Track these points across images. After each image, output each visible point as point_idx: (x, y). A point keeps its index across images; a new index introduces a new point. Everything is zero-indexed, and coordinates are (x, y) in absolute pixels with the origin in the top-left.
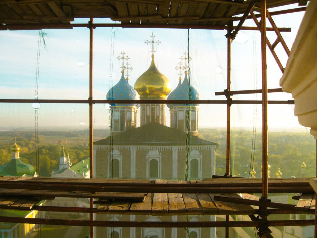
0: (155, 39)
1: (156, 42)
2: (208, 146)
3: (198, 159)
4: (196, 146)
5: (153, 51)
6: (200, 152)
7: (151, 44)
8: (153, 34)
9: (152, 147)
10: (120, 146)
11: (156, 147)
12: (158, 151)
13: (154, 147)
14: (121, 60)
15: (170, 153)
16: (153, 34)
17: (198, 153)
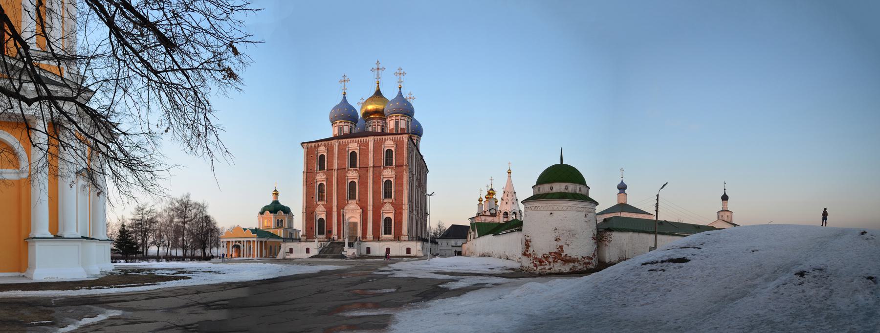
0: (380, 66)
1: (381, 69)
2: (402, 136)
3: (393, 149)
4: (390, 136)
5: (378, 77)
6: (394, 141)
7: (376, 72)
8: (378, 62)
9: (351, 139)
10: (325, 142)
11: (354, 139)
12: (356, 143)
13: (353, 139)
14: (343, 83)
15: (367, 144)
16: (378, 62)
17: (393, 143)
